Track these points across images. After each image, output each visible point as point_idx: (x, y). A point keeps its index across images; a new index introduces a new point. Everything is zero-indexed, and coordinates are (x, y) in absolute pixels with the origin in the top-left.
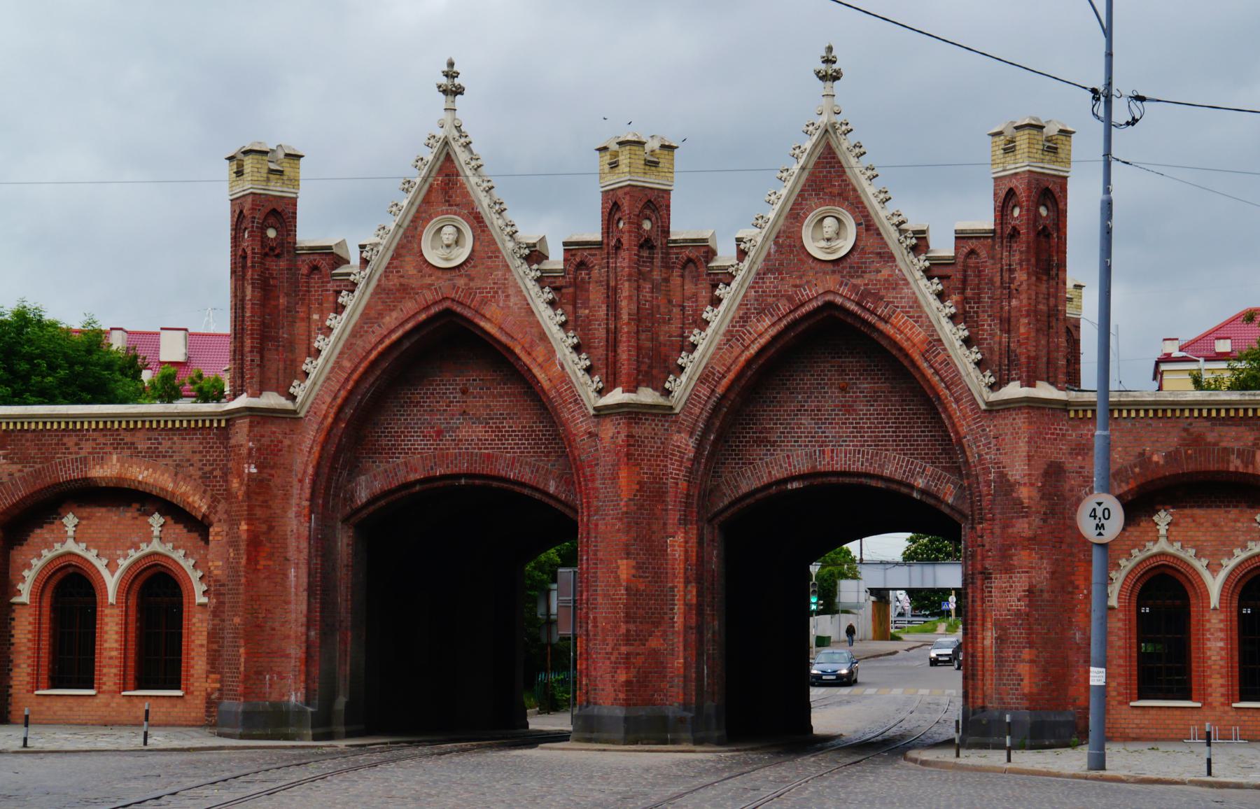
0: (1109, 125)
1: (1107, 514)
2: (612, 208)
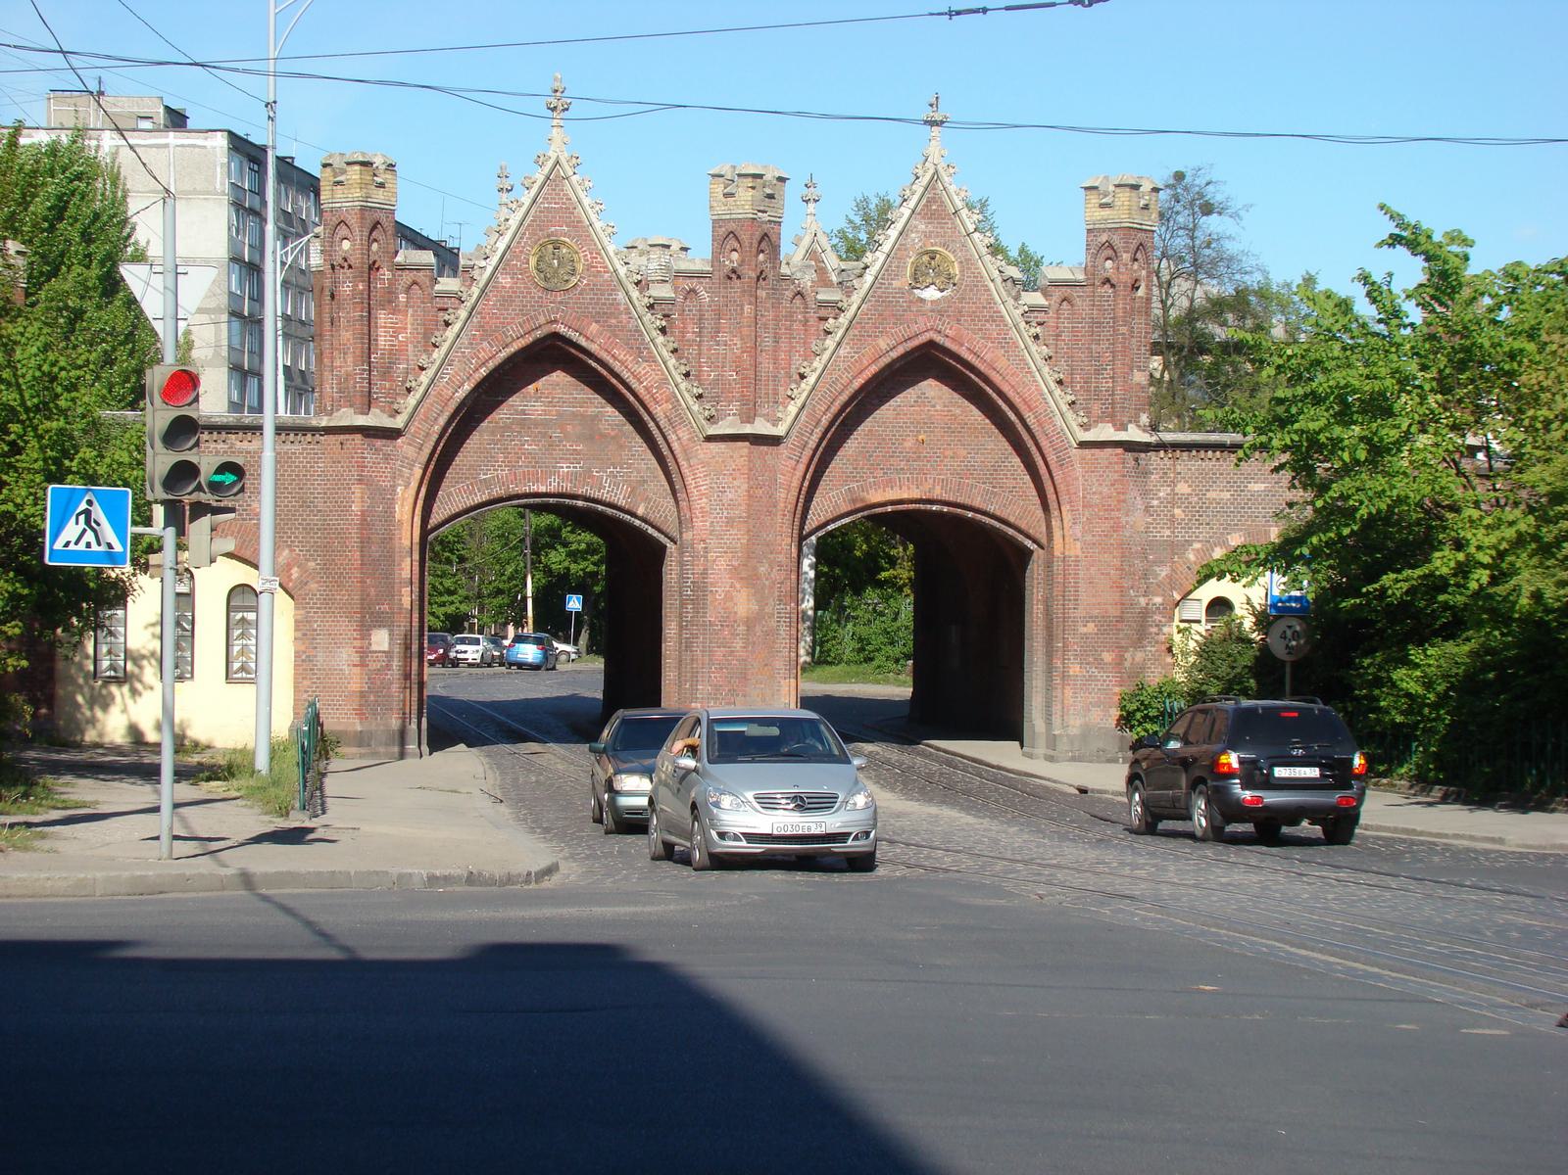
2: (726, 235)
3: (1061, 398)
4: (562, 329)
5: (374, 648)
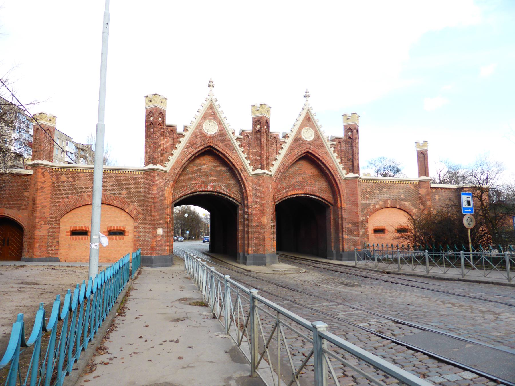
3: (341, 166)
4: (212, 145)
5: (158, 234)
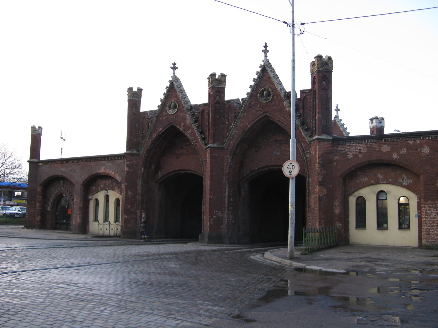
0: (294, 35)
1: (293, 167)
